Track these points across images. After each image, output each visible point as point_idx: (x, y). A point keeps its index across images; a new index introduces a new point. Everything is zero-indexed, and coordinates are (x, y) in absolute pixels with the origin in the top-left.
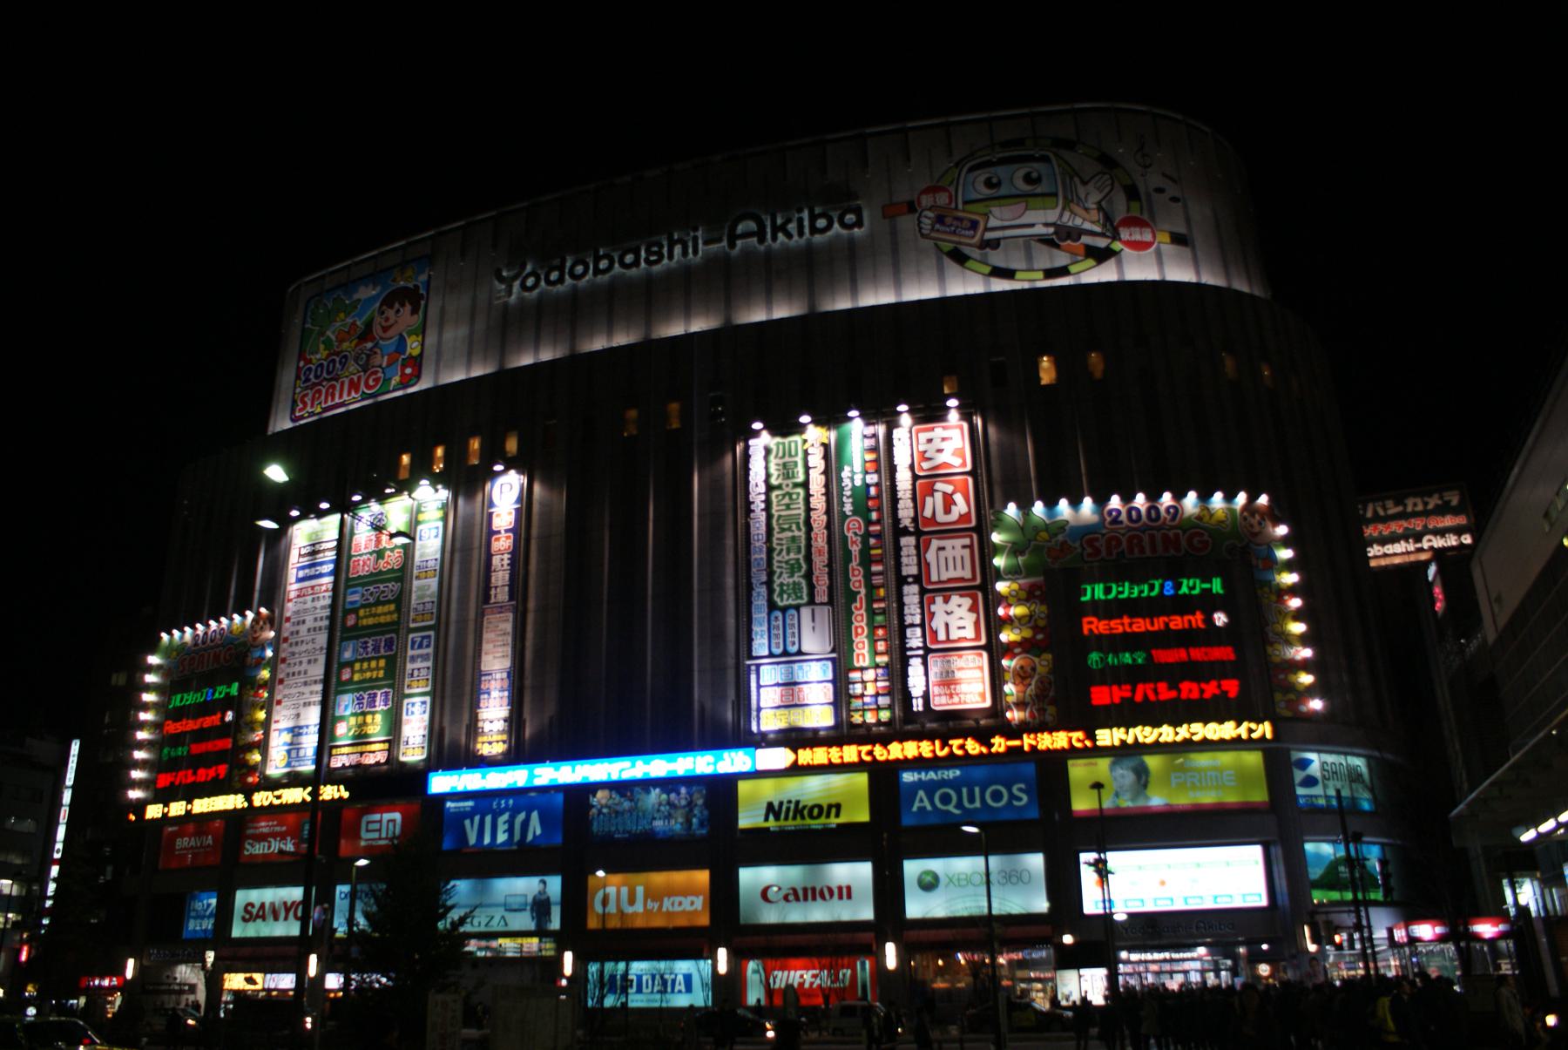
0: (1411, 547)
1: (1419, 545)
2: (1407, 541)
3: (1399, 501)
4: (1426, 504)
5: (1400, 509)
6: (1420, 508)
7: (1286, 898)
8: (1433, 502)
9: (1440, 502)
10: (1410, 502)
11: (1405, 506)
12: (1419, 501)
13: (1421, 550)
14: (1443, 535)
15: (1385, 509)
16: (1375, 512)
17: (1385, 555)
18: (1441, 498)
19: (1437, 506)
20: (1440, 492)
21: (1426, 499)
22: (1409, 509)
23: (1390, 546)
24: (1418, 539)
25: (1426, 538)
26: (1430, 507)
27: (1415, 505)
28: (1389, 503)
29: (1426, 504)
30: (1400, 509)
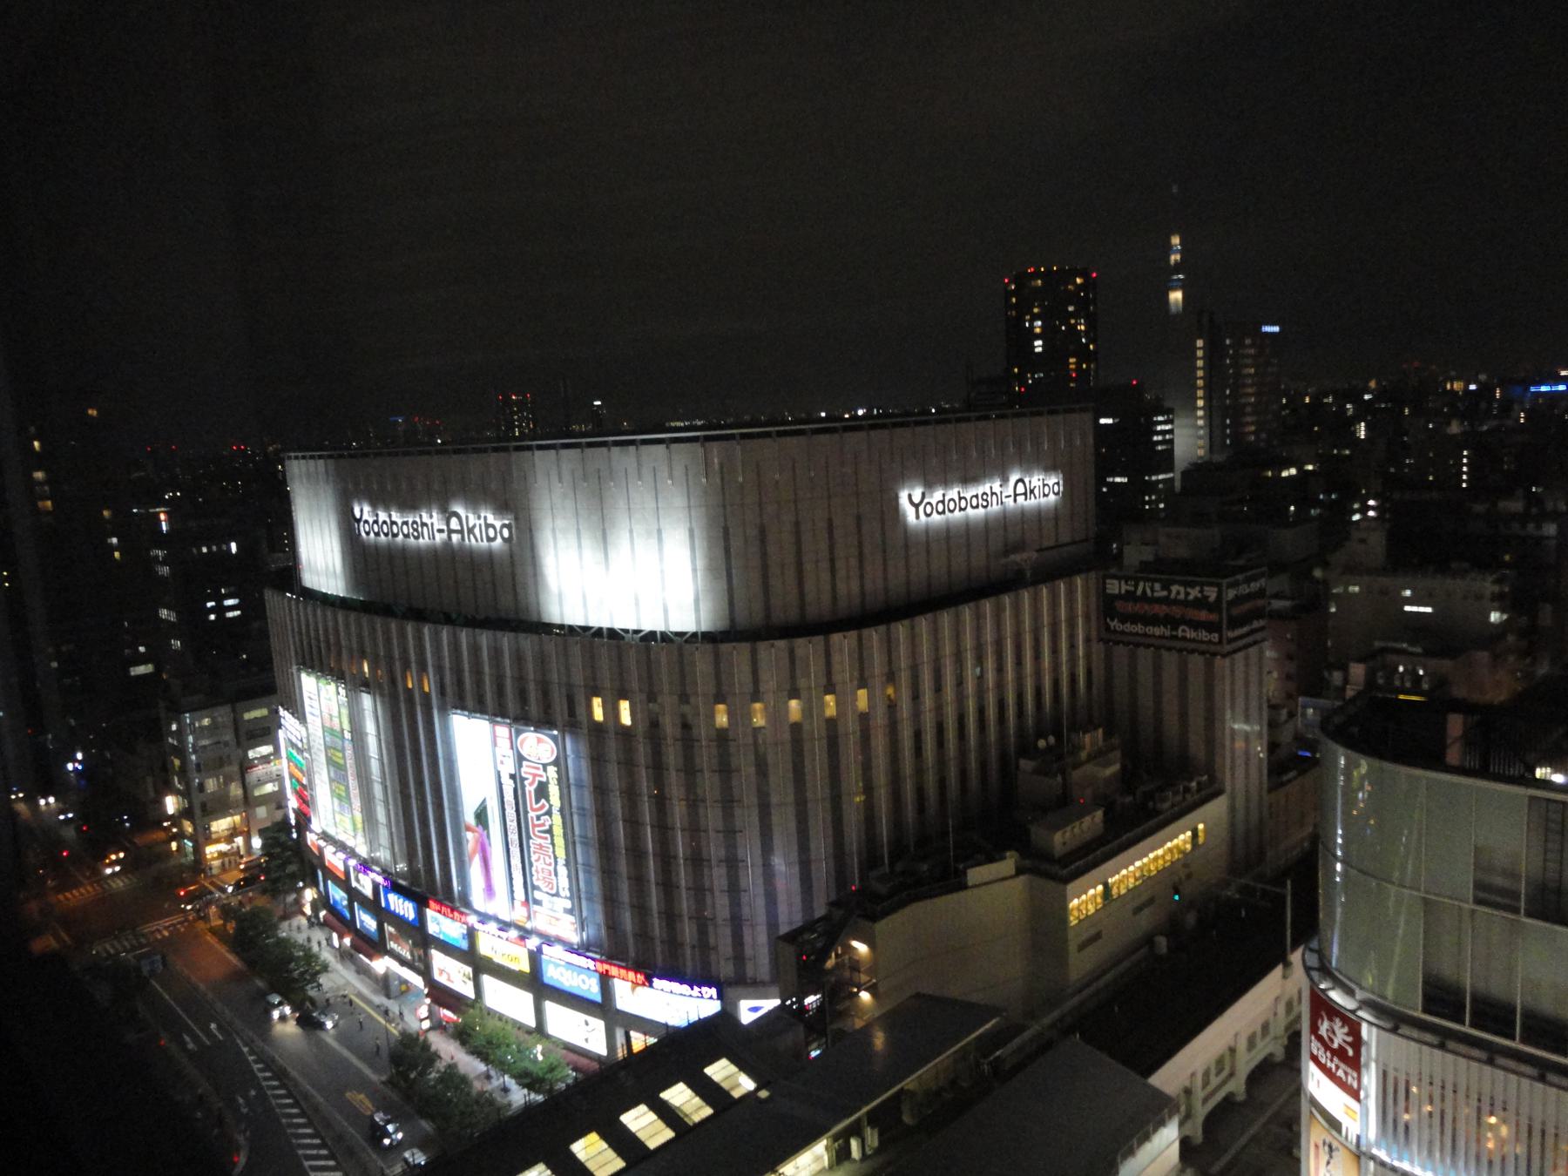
0: (1168, 633)
1: (1174, 633)
2: (1165, 626)
3: (1166, 587)
4: (1187, 594)
5: (1165, 593)
6: (1182, 596)
7: (697, 1101)
8: (1194, 593)
9: (1199, 595)
10: (1175, 588)
11: (1170, 591)
12: (1182, 589)
13: (1175, 638)
14: (1196, 629)
15: (1153, 590)
16: (1144, 591)
17: (1145, 635)
18: (1201, 591)
19: (1196, 598)
20: (1202, 585)
21: (1189, 590)
22: (1173, 596)
23: (1151, 628)
24: (1175, 628)
25: (1181, 628)
26: (1191, 597)
27: (1178, 593)
28: (1157, 586)
29: (1187, 594)
30: (1165, 593)
